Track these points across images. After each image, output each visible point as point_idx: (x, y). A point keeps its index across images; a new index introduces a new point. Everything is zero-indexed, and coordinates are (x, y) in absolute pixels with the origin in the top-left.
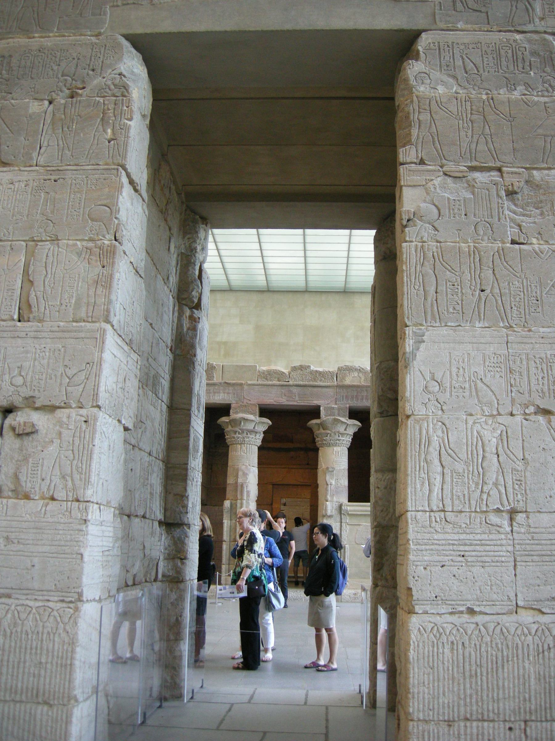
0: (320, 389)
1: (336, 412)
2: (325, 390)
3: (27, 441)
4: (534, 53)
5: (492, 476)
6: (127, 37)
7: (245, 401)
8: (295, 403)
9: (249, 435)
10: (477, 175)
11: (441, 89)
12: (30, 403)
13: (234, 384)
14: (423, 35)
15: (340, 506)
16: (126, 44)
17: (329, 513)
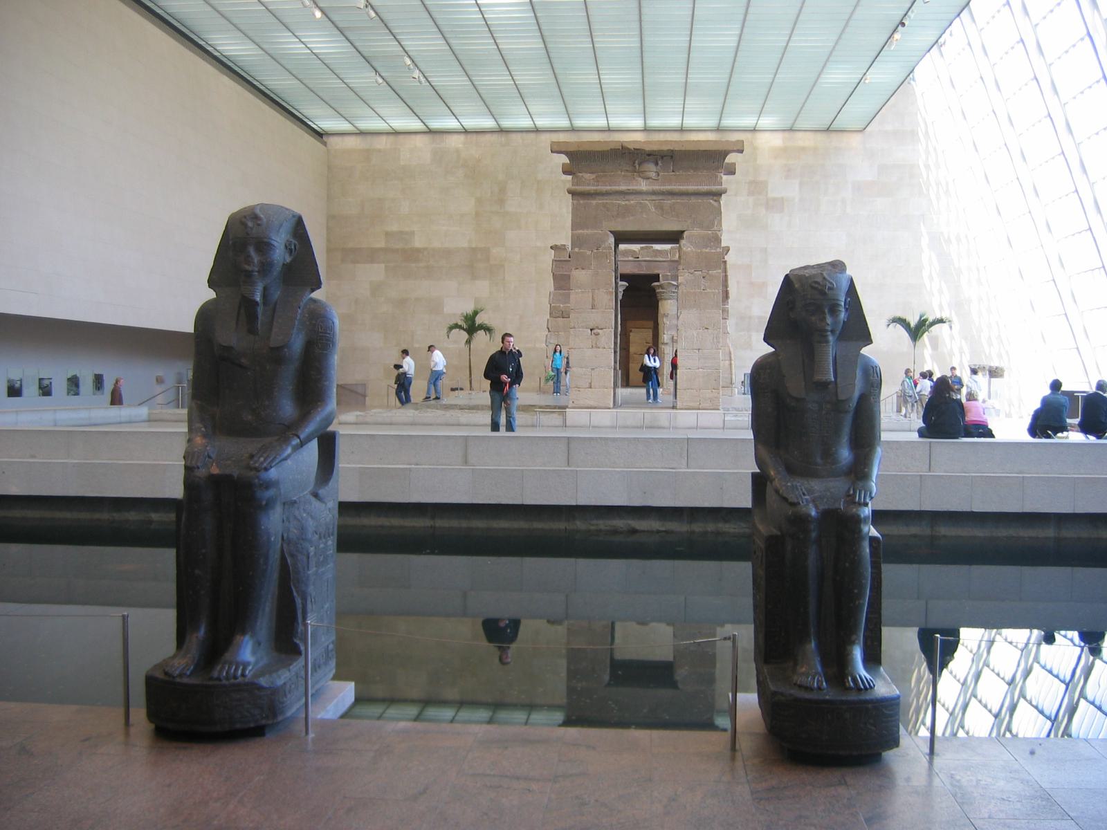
2: (663, 263)
12: (598, 328)
14: (686, 232)
17: (666, 341)
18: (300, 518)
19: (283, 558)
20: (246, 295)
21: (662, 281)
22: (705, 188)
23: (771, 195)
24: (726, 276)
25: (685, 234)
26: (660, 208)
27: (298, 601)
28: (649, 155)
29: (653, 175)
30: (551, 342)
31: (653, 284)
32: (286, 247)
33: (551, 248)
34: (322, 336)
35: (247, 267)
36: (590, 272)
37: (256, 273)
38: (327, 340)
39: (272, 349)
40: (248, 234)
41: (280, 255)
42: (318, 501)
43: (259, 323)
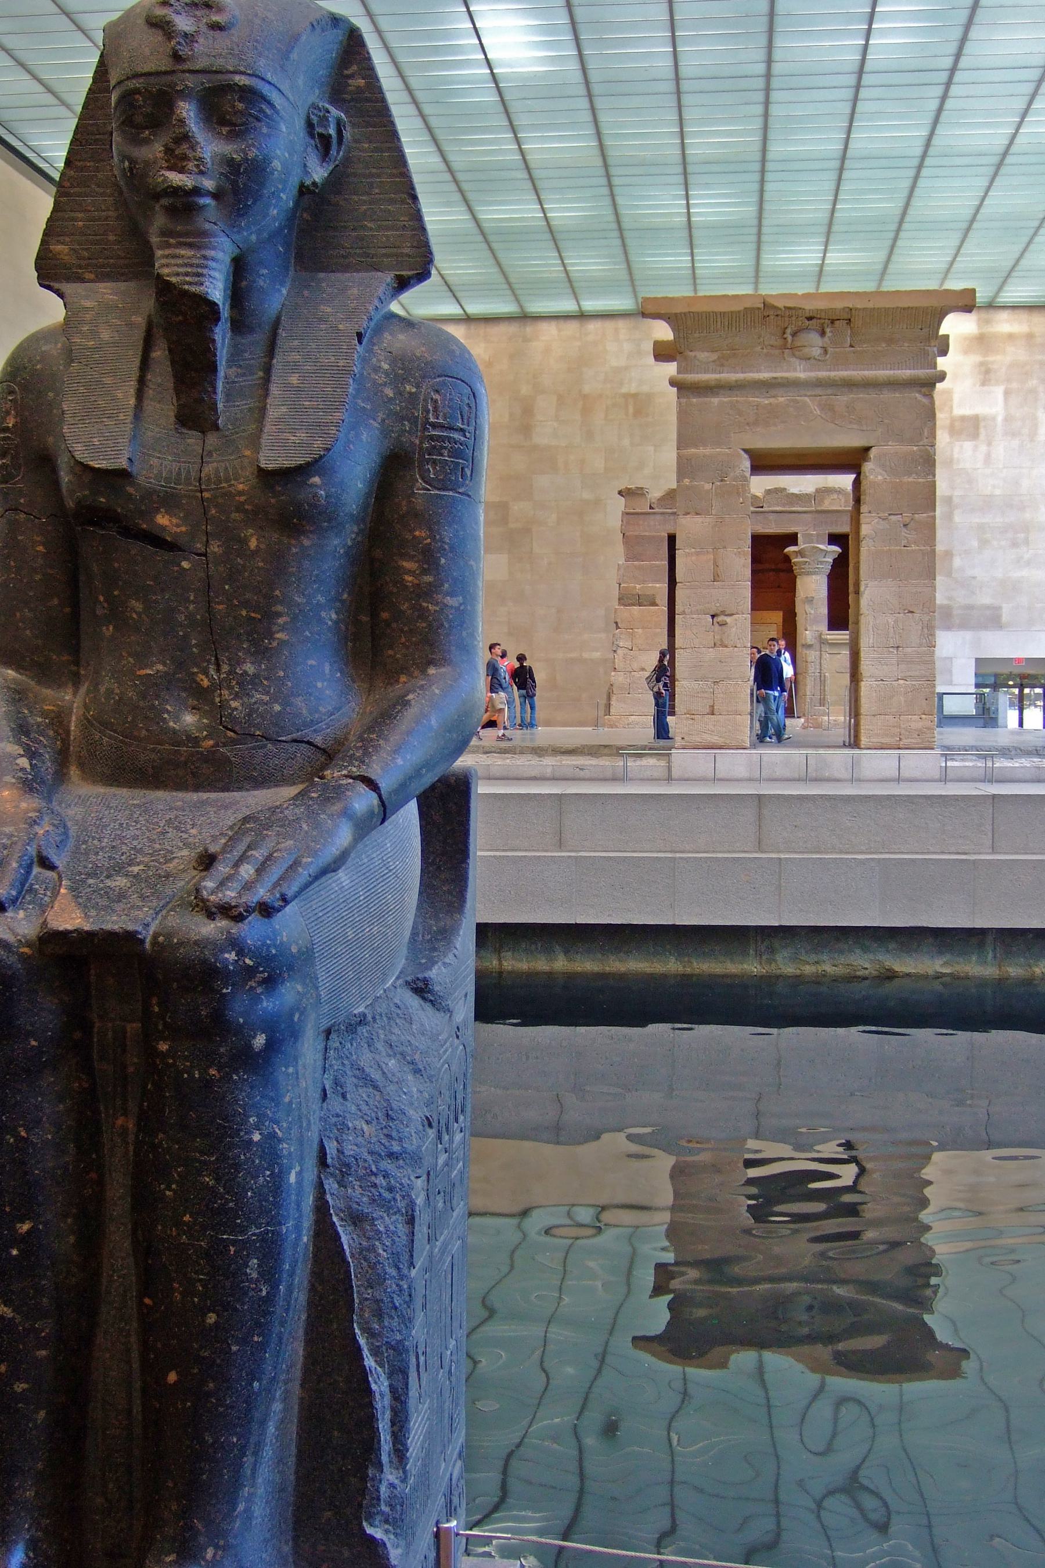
1: (815, 538)
3: (724, 627)
4: (921, 457)
5: (891, 635)
6: (744, 450)
10: (892, 517)
11: (880, 477)
12: (723, 613)
16: (742, 453)
17: (809, 642)
18: (376, 1075)
19: (324, 1232)
20: (173, 280)
21: (802, 544)
22: (906, 373)
23: (958, 411)
25: (872, 453)
26: (829, 408)
27: (380, 1385)
28: (810, 319)
29: (816, 352)
30: (621, 644)
31: (787, 550)
32: (310, 125)
33: (620, 493)
34: (439, 438)
35: (176, 178)
36: (708, 520)
37: (207, 201)
38: (456, 454)
39: (264, 474)
40: (177, 57)
41: (289, 156)
42: (428, 1006)
43: (220, 385)
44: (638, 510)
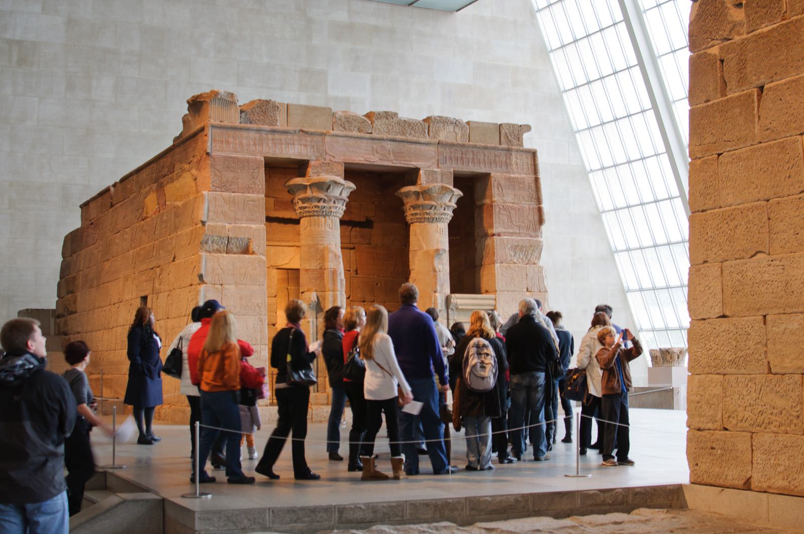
0: (418, 146)
1: (439, 178)
2: (423, 147)
7: (328, 158)
8: (390, 164)
9: (336, 205)
13: (312, 134)
15: (448, 301)
24: (537, 180)
44: (226, 123)
